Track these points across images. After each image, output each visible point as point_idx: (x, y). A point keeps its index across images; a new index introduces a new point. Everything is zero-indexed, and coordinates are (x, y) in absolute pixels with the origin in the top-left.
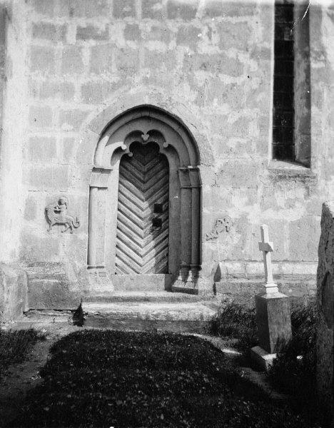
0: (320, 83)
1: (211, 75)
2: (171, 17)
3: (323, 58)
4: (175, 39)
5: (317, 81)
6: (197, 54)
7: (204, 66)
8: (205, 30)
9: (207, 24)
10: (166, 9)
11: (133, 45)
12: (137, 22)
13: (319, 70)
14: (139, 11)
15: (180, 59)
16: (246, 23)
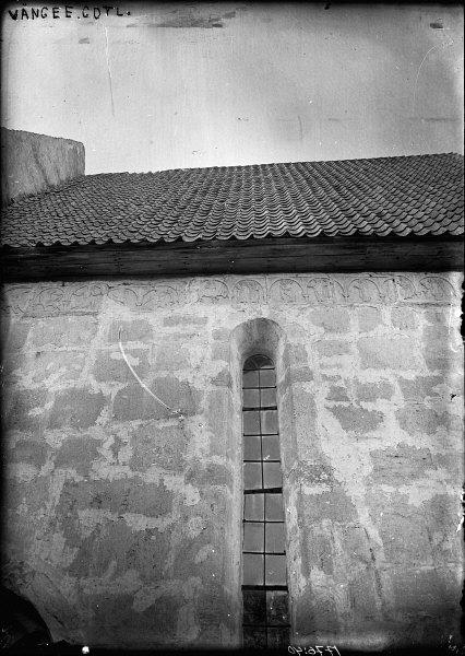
0: (325, 522)
1: (109, 515)
4: (54, 458)
5: (317, 519)
7: (98, 502)
8: (111, 441)
13: (318, 499)
15: (56, 490)
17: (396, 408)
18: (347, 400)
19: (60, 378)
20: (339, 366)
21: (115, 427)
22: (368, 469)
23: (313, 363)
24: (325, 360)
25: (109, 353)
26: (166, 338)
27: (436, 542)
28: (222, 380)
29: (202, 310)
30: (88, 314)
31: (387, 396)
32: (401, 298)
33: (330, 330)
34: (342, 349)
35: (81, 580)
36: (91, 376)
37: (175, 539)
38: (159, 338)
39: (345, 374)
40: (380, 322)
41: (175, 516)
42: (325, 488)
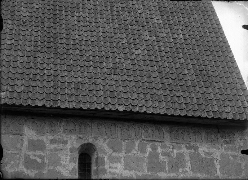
19: (12, 166)
23: (107, 167)
24: (111, 165)
25: (29, 155)
26: (51, 150)
29: (65, 137)
30: (18, 134)
32: (143, 138)
33: (114, 151)
34: (118, 160)
36: (23, 167)
38: (49, 150)
40: (134, 148)
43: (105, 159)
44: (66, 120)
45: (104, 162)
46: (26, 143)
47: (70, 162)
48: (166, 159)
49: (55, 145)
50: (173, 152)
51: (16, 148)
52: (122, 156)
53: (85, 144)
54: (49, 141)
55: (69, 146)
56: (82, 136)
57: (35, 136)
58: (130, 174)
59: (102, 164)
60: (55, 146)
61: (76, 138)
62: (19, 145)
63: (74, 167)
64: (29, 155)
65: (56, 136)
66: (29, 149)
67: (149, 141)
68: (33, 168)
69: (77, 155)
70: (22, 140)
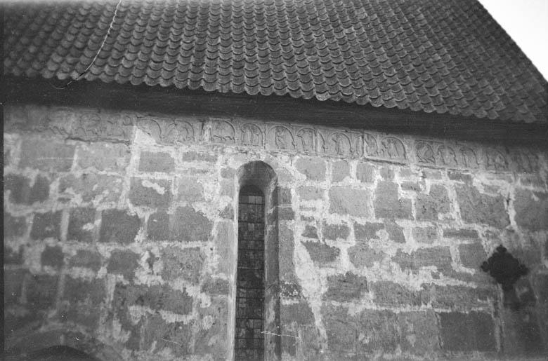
0: (293, 324)
1: (150, 311)
2: (104, 238)
3: (296, 292)
4: (106, 265)
5: (289, 322)
6: (132, 284)
7: (141, 300)
8: (146, 256)
9: (149, 250)
10: (98, 233)
11: (49, 270)
12: (60, 244)
13: (291, 308)
14: (64, 233)
15: (111, 288)
16: (198, 249)
17: (349, 246)
18: (316, 236)
19: (105, 198)
20: (314, 209)
21: (149, 245)
22: (324, 290)
23: (295, 205)
24: (305, 203)
25: (140, 180)
26: (185, 172)
27: (360, 339)
28: (226, 213)
30: (122, 142)
31: (345, 237)
34: (318, 194)
35: (135, 352)
36: (128, 200)
37: (195, 330)
39: (317, 215)
40: (348, 174)
41: (194, 315)
42: (296, 301)
43: (292, 190)
44: (215, 119)
45: (290, 197)
46: (135, 158)
47: (222, 194)
48: (412, 196)
49: (192, 163)
50: (424, 183)
51: (116, 167)
52: (326, 186)
53: (251, 163)
54: (181, 157)
55: (219, 166)
56: (246, 148)
57: (155, 146)
58: (343, 221)
59: (285, 201)
60: (194, 164)
61: (235, 152)
62: (121, 161)
63: (230, 205)
64: (140, 180)
65: (196, 148)
66: (142, 168)
67: (377, 161)
68: (148, 204)
69: (237, 186)
70: (129, 152)
